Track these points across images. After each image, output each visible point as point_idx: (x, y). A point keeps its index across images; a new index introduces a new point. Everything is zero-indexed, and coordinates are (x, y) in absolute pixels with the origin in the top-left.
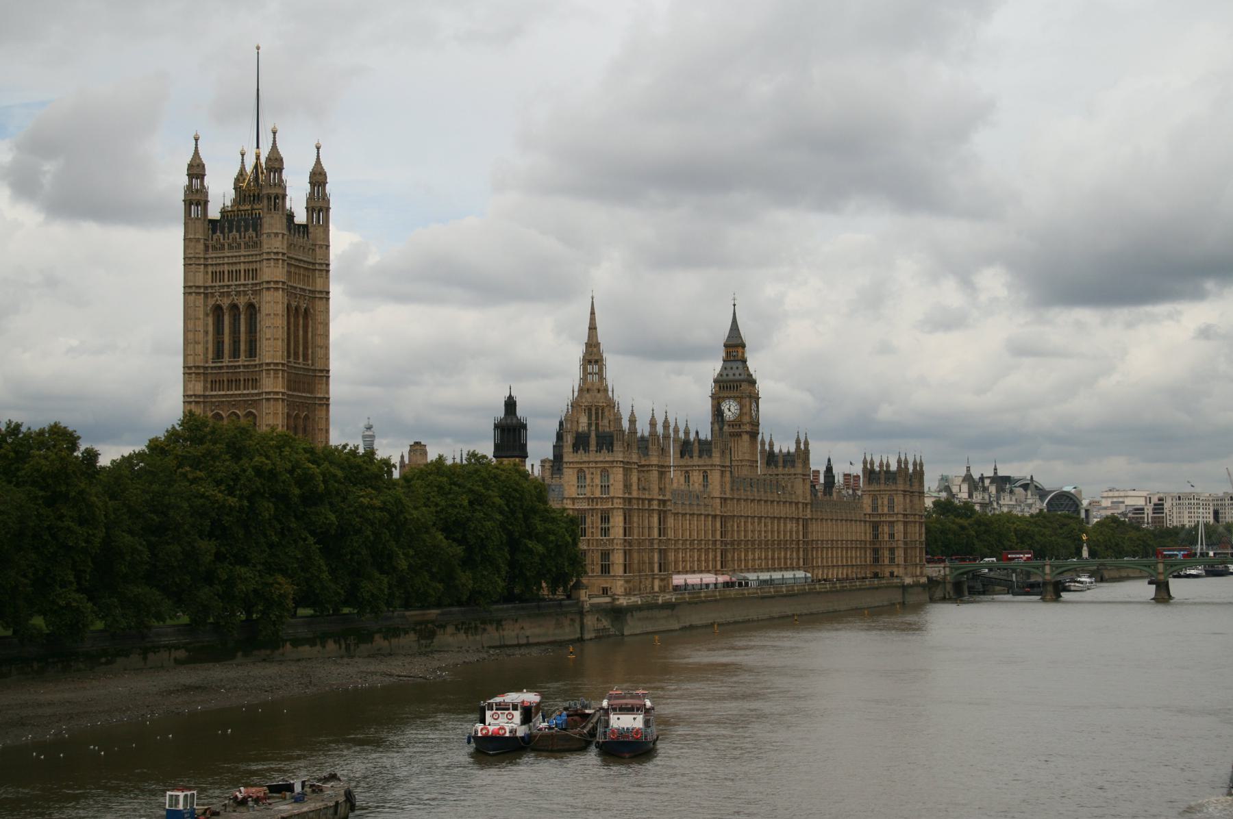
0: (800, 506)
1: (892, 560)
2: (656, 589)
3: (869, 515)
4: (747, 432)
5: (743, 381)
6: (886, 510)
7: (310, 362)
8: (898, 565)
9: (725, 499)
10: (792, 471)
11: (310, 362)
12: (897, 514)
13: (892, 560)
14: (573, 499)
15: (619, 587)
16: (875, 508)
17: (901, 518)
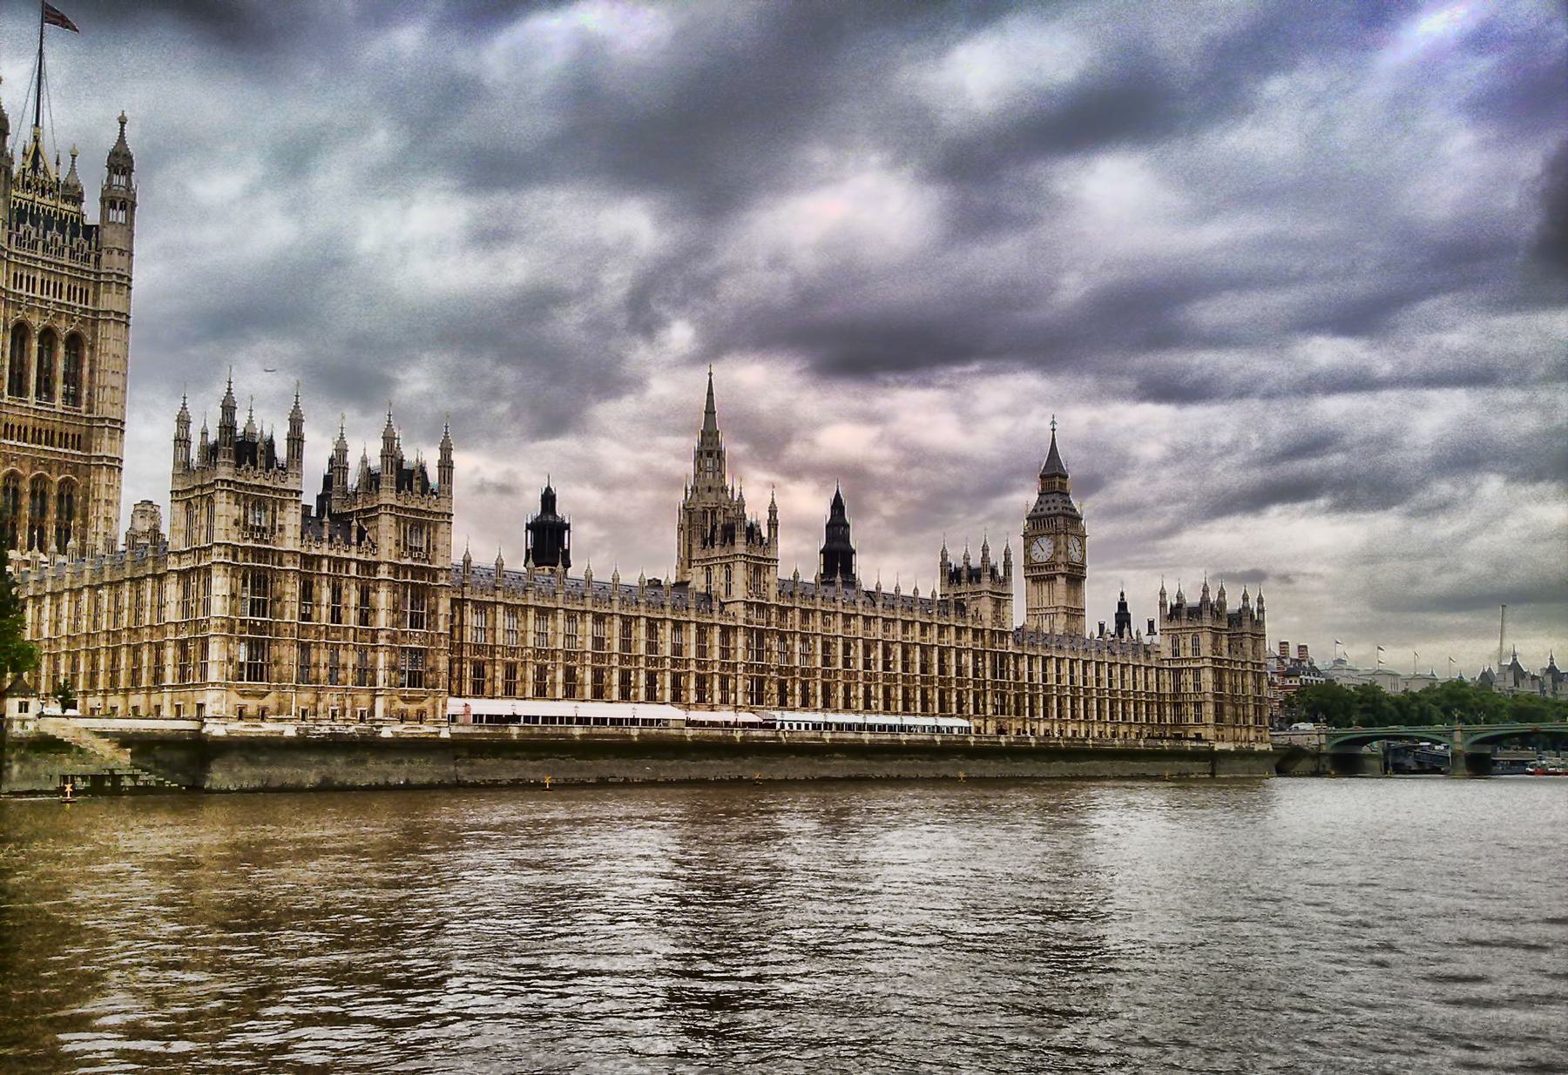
0: (986, 633)
1: (1198, 718)
2: (379, 714)
3: (1169, 660)
4: (1063, 575)
5: (1058, 514)
6: (1189, 654)
7: (83, 408)
8: (1206, 724)
9: (761, 607)
10: (978, 588)
11: (83, 408)
12: (1202, 658)
13: (1198, 718)
14: (179, 554)
15: (214, 702)
16: (1176, 653)
17: (1208, 663)
